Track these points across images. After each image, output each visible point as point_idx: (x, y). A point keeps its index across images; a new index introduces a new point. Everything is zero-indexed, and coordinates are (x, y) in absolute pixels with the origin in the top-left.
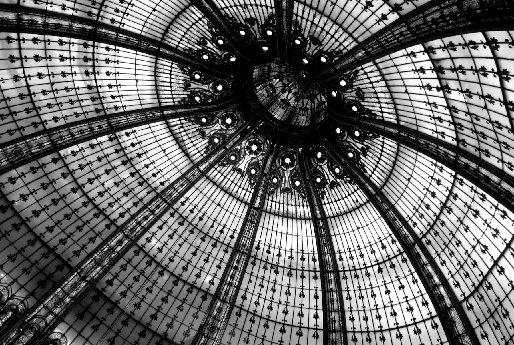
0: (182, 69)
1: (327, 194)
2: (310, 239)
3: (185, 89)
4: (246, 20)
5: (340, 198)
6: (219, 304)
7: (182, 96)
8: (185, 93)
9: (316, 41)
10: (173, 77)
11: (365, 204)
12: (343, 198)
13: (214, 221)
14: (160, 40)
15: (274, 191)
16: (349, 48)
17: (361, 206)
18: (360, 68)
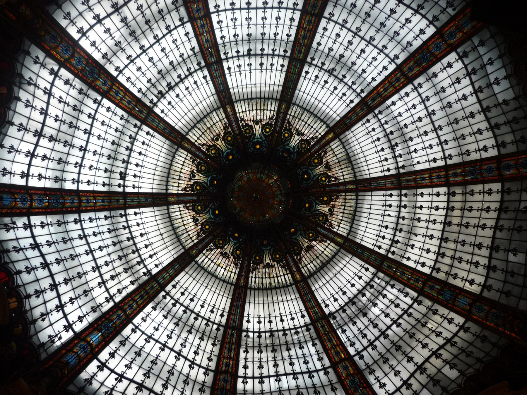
0: (255, 269)
1: (311, 136)
2: (355, 133)
3: (273, 266)
4: (196, 225)
5: (307, 125)
6: (452, 179)
7: (280, 269)
8: (276, 266)
9: (192, 175)
10: (264, 276)
11: (298, 106)
12: (306, 123)
13: (384, 215)
14: (233, 287)
15: (334, 177)
16: (186, 153)
17: (301, 107)
18: (196, 143)
